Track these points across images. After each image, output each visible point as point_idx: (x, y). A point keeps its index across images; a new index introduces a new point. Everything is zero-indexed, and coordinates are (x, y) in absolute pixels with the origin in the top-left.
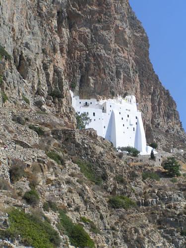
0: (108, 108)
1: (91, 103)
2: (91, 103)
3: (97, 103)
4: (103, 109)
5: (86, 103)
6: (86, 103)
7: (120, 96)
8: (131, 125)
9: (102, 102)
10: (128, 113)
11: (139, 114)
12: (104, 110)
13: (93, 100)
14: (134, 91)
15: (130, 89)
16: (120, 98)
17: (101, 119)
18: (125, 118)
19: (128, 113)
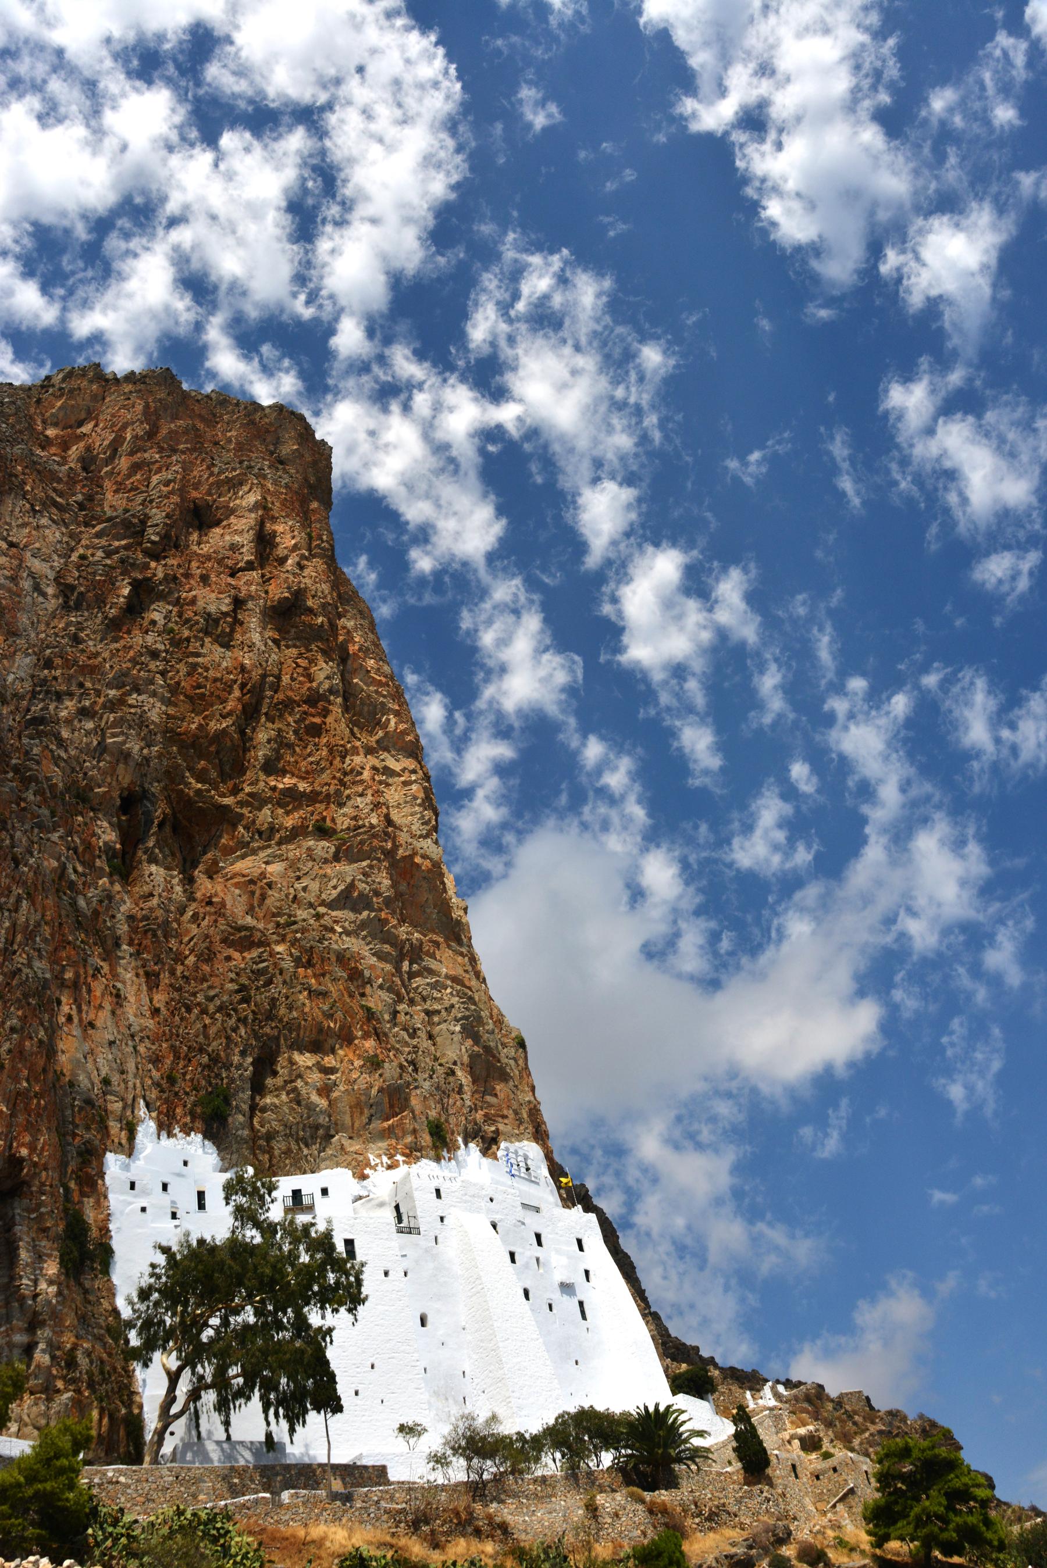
0: (425, 1209)
1: (325, 1192)
2: (325, 1192)
3: (355, 1187)
4: (399, 1218)
5: (297, 1194)
6: (297, 1194)
7: (472, 1145)
8: (567, 1288)
9: (383, 1181)
10: (534, 1222)
11: (587, 1224)
12: (404, 1222)
13: (338, 1178)
14: (531, 1129)
15: (510, 1113)
16: (471, 1154)
17: (396, 1274)
18: (527, 1251)
19: (534, 1222)
